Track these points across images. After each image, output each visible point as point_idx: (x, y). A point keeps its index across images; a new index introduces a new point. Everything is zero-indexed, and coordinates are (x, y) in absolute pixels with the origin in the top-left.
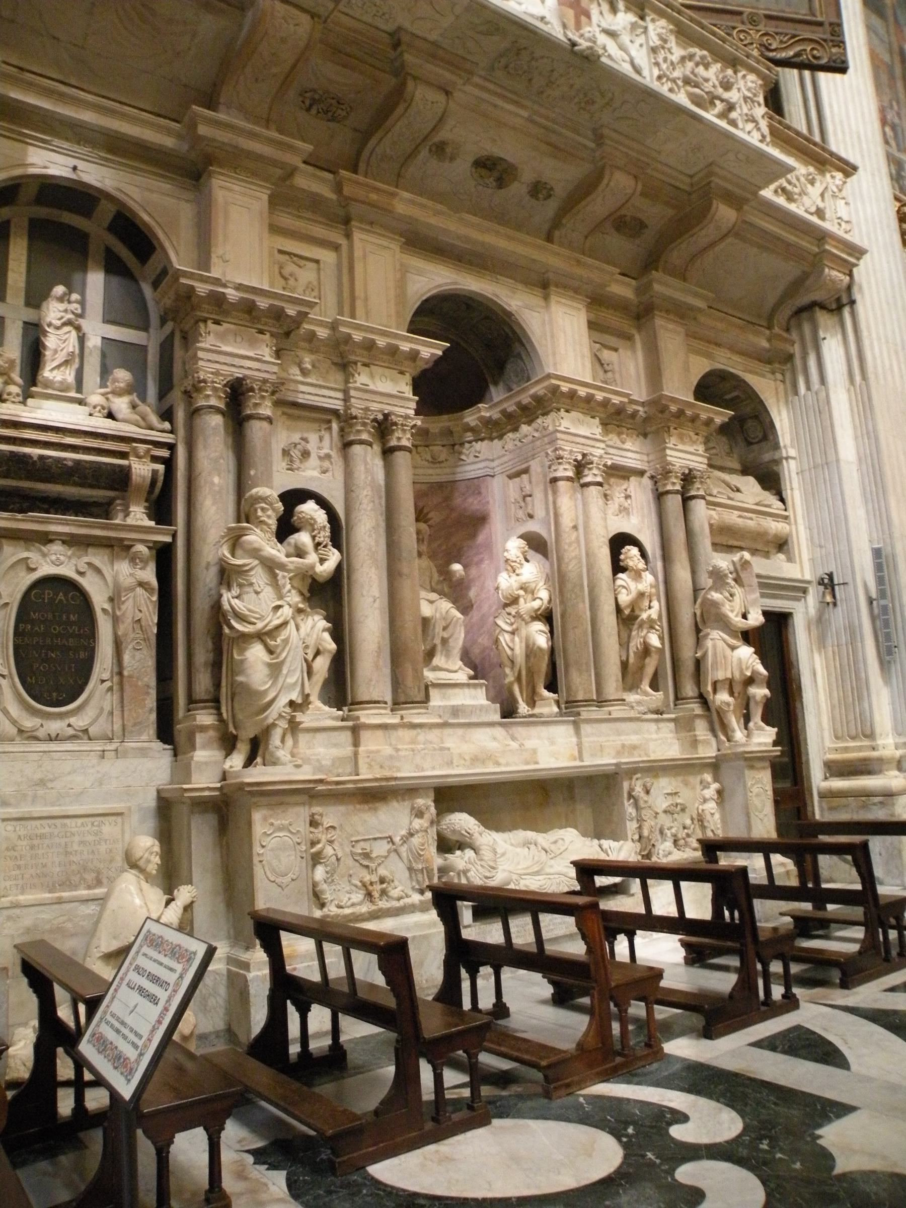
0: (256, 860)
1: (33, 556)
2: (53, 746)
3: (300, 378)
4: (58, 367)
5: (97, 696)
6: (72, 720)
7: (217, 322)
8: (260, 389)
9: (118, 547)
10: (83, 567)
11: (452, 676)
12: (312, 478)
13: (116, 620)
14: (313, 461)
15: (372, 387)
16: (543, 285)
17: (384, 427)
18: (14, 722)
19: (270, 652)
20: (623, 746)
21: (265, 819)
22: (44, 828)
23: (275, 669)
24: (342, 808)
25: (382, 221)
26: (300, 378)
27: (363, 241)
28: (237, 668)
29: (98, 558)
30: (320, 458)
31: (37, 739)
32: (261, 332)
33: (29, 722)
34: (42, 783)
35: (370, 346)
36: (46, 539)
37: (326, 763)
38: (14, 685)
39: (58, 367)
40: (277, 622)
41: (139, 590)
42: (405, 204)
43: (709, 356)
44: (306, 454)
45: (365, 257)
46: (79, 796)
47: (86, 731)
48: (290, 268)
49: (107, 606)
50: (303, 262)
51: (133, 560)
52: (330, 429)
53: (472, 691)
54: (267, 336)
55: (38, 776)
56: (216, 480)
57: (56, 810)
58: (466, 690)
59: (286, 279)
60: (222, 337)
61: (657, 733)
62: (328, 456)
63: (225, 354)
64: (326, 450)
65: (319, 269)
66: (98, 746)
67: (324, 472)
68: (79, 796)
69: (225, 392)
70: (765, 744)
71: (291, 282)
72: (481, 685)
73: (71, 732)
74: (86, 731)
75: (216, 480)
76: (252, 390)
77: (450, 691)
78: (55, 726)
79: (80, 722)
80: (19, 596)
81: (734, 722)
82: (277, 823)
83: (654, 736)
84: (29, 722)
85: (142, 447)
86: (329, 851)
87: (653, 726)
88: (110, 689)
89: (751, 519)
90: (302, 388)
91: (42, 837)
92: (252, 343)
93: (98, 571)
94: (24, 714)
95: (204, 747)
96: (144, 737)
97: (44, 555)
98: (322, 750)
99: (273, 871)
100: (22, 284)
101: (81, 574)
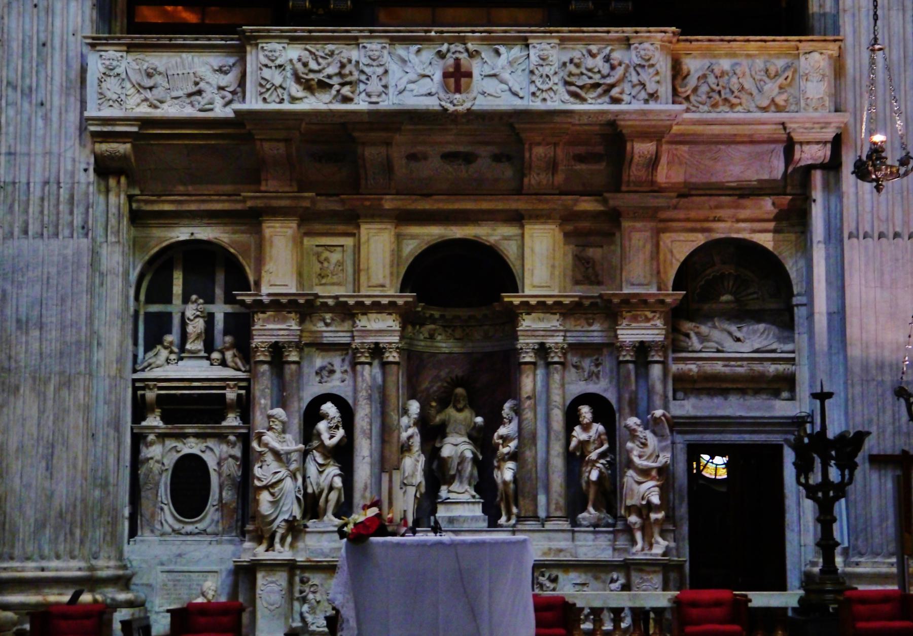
0: (257, 596)
1: (179, 445)
2: (189, 538)
3: (325, 329)
4: (194, 341)
5: (211, 514)
6: (198, 525)
7: (263, 312)
8: (289, 347)
9: (221, 437)
10: (203, 449)
11: (460, 496)
12: (333, 387)
13: (220, 475)
14: (338, 375)
15: (369, 328)
16: (517, 218)
17: (377, 351)
18: (170, 526)
19: (272, 494)
20: (550, 549)
21: (264, 577)
22: (180, 577)
23: (275, 503)
24: (323, 576)
25: (377, 215)
26: (325, 329)
27: (366, 230)
28: (257, 502)
29: (211, 443)
30: (342, 373)
31: (181, 534)
32: (290, 312)
33: (177, 526)
34: (180, 555)
35: (360, 304)
36: (186, 436)
37: (327, 551)
38: (170, 509)
39: (194, 341)
40: (274, 481)
41: (230, 460)
42: (389, 203)
43: (704, 230)
44: (332, 372)
45: (368, 240)
46: (198, 562)
47: (205, 530)
48: (326, 254)
49: (216, 468)
50: (333, 249)
51: (228, 443)
52: (347, 354)
53: (471, 506)
54: (293, 315)
55: (178, 552)
56: (263, 401)
57: (185, 568)
58: (466, 506)
59: (322, 263)
60: (267, 321)
61: (594, 540)
62: (346, 371)
63: (268, 330)
64: (345, 367)
65: (343, 251)
66: (209, 538)
67: (343, 381)
68: (198, 562)
69: (270, 352)
70: (656, 555)
71: (326, 264)
72: (478, 502)
73: (197, 531)
74: (205, 530)
75: (263, 401)
76: (284, 347)
77: (454, 507)
78: (189, 528)
79: (201, 526)
80: (172, 465)
81: (638, 536)
82: (269, 579)
83: (591, 543)
84: (177, 526)
85: (231, 383)
86: (311, 596)
87: (591, 536)
88: (217, 510)
89: (741, 366)
90: (325, 334)
91: (179, 581)
92: (284, 320)
93: (212, 450)
94: (175, 522)
95: (250, 540)
96: (234, 534)
97: (184, 444)
98: (326, 544)
99: (268, 603)
100: (180, 292)
101: (203, 452)
